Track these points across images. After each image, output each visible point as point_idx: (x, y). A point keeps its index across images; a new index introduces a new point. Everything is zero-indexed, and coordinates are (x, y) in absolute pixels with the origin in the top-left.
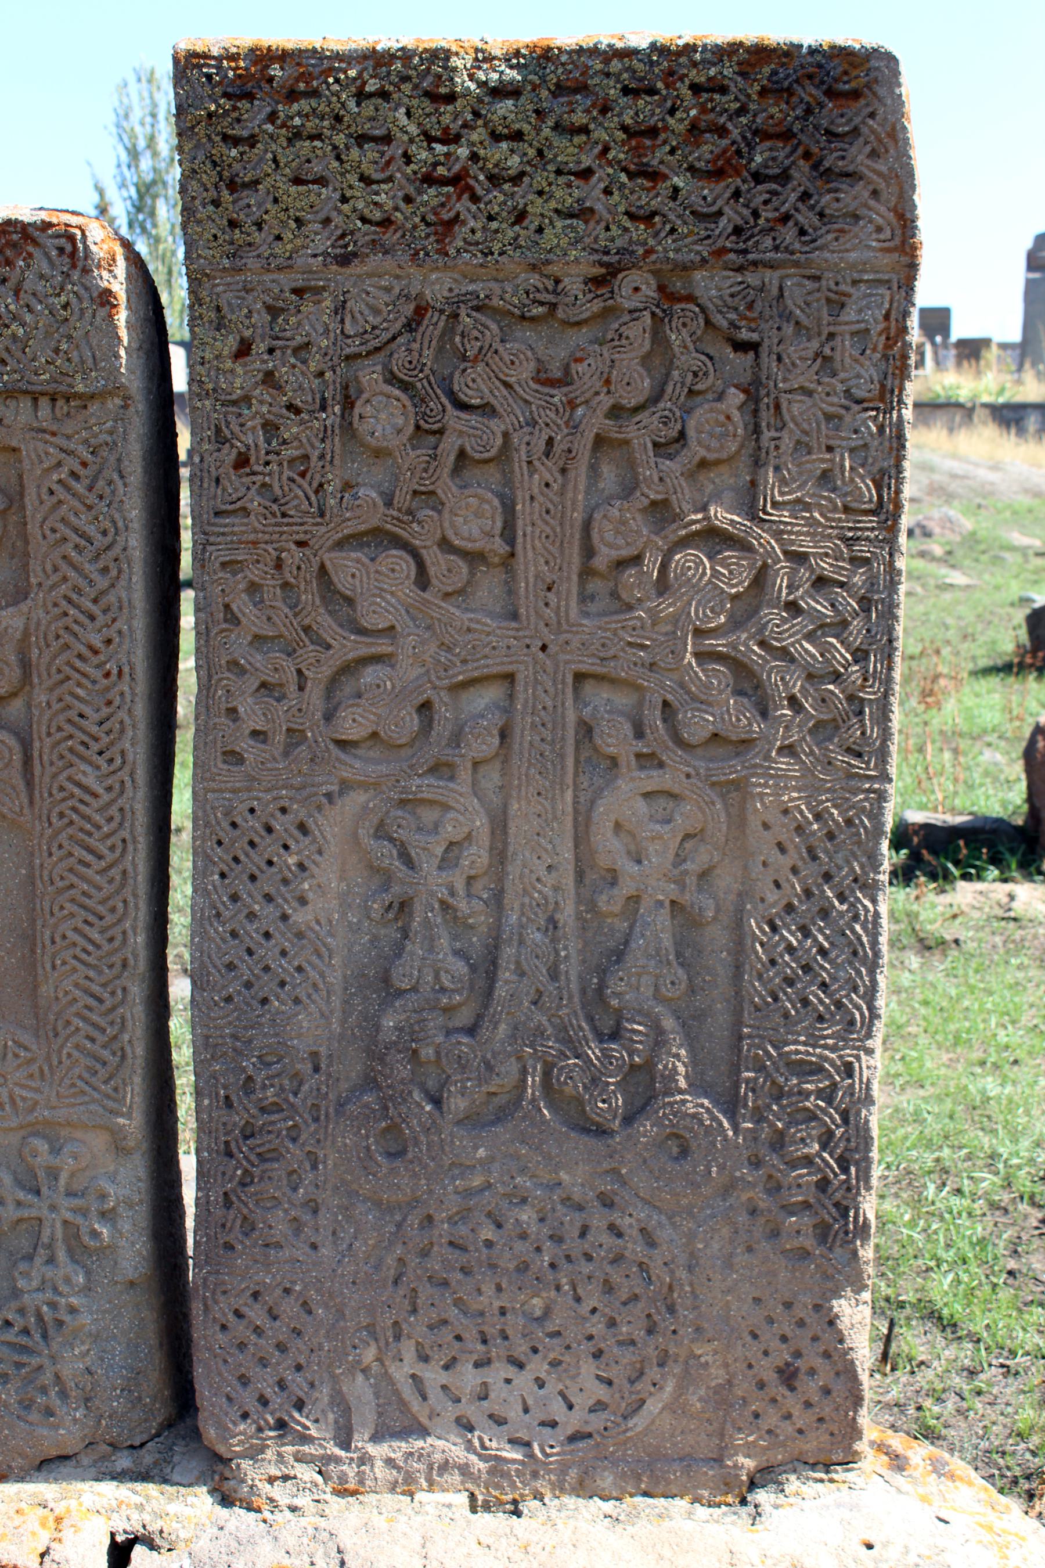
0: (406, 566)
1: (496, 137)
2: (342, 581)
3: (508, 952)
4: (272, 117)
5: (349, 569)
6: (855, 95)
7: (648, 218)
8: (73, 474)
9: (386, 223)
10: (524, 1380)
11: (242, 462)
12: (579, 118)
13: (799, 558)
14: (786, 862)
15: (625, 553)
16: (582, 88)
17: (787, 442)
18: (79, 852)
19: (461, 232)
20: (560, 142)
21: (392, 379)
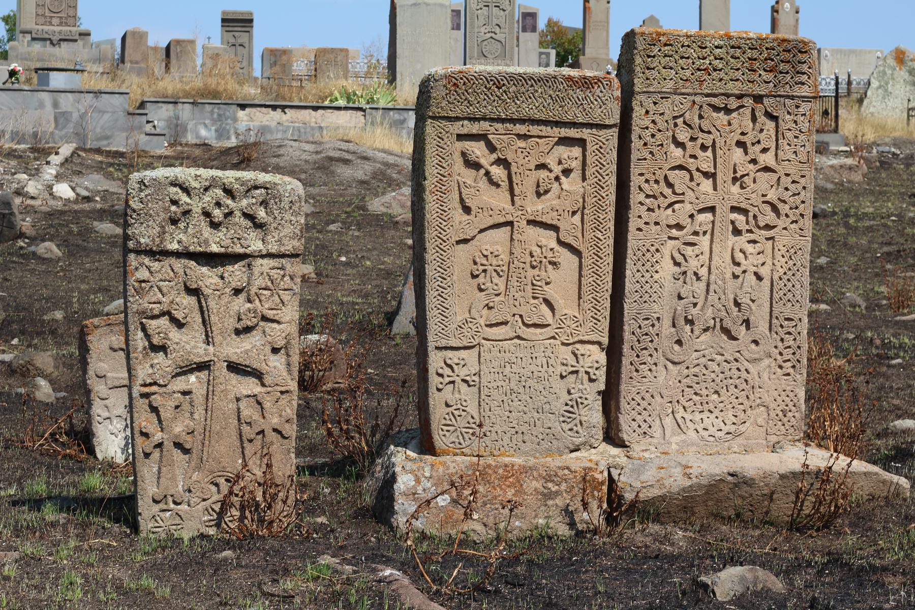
0: (688, 176)
1: (716, 59)
2: (671, 180)
3: (712, 287)
4: (660, 50)
5: (674, 176)
6: (806, 52)
7: (753, 82)
8: (601, 147)
9: (686, 80)
10: (713, 416)
11: (645, 144)
12: (737, 55)
13: (787, 175)
14: (784, 260)
15: (745, 173)
16: (739, 48)
17: (785, 142)
18: (596, 257)
19: (705, 83)
20: (732, 60)
21: (685, 123)
